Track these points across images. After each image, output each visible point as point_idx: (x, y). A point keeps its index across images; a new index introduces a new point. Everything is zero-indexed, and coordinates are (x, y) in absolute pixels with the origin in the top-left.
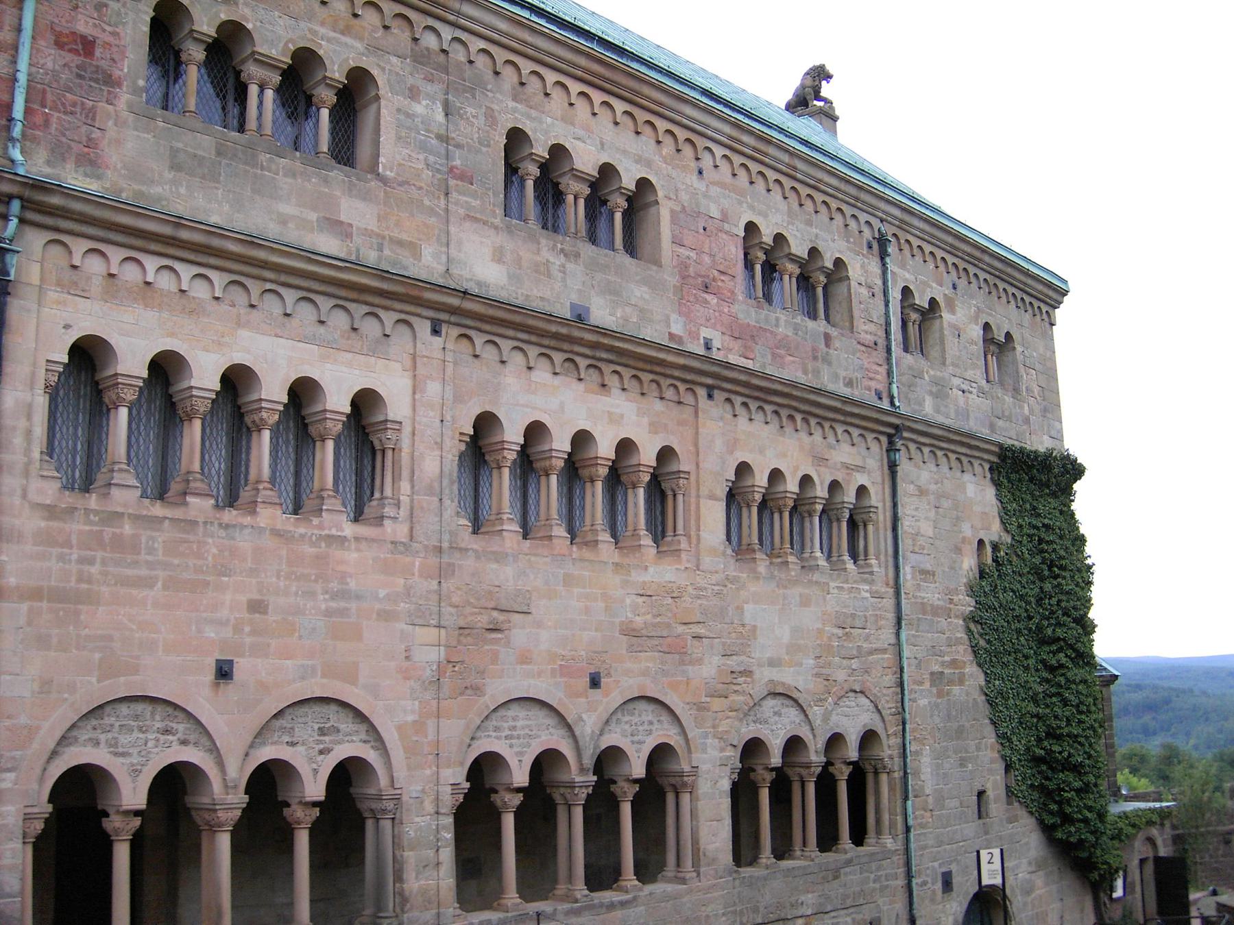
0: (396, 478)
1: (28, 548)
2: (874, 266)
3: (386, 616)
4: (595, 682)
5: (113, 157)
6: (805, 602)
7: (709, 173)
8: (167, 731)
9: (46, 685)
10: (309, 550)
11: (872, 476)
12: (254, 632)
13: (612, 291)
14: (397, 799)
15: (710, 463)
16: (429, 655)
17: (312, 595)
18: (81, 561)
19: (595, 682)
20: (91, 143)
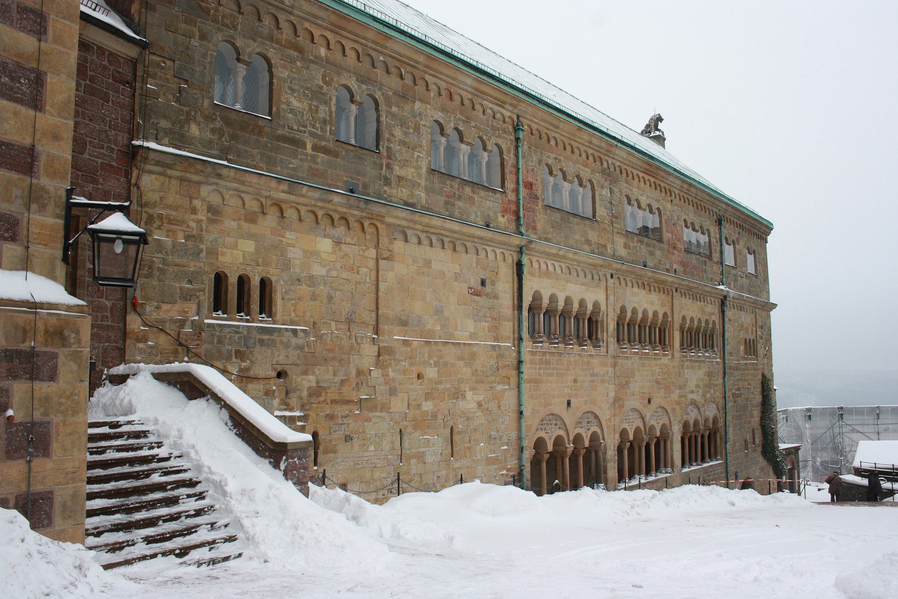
0: (602, 331)
1: (529, 366)
2: (717, 229)
3: (603, 381)
4: (649, 401)
5: (539, 226)
6: (700, 368)
7: (675, 202)
8: (556, 425)
9: (533, 410)
10: (586, 360)
11: (716, 318)
12: (575, 390)
13: (652, 254)
14: (605, 446)
15: (676, 317)
16: (612, 394)
17: (586, 375)
18: (540, 369)
19: (649, 401)
20: (534, 221)
